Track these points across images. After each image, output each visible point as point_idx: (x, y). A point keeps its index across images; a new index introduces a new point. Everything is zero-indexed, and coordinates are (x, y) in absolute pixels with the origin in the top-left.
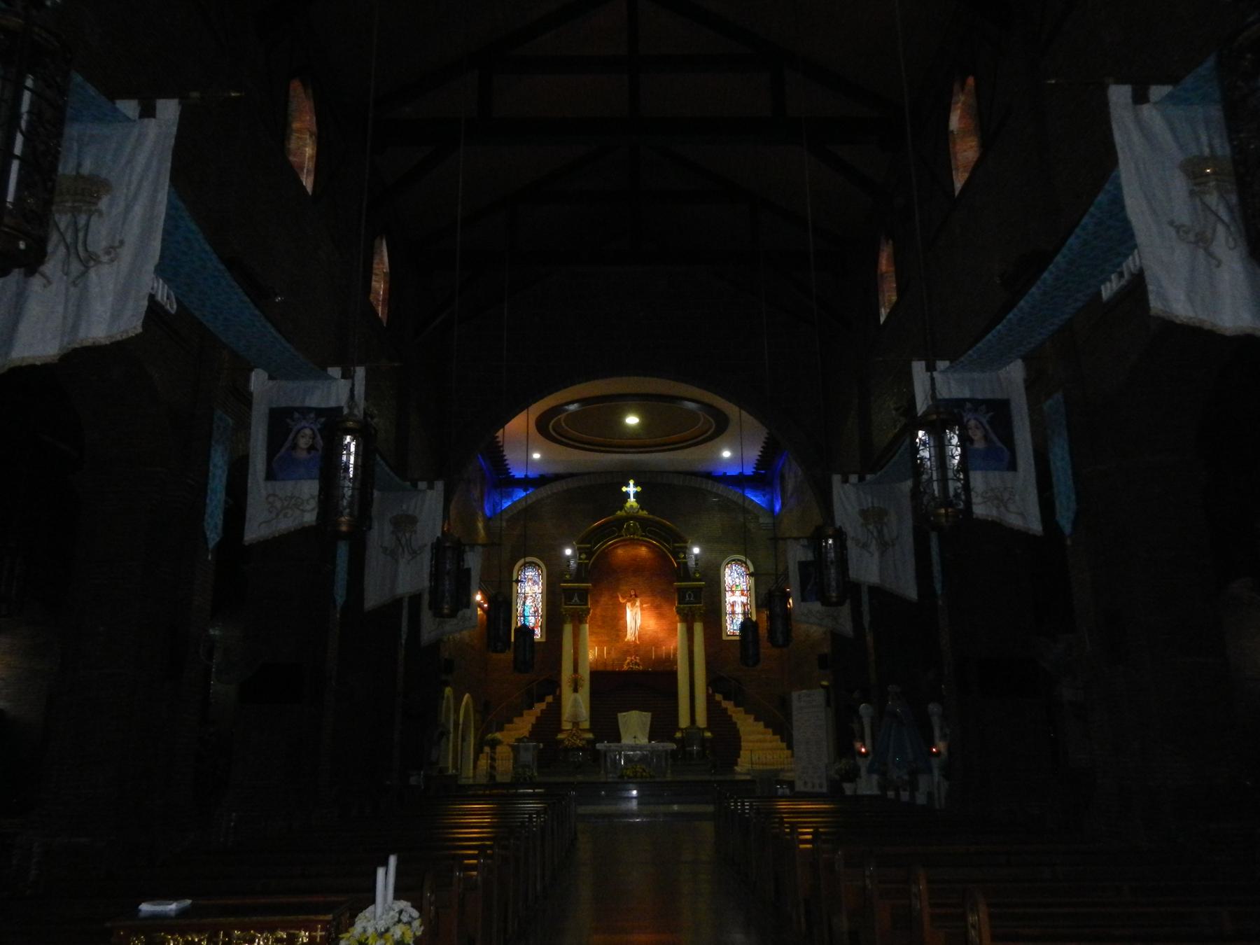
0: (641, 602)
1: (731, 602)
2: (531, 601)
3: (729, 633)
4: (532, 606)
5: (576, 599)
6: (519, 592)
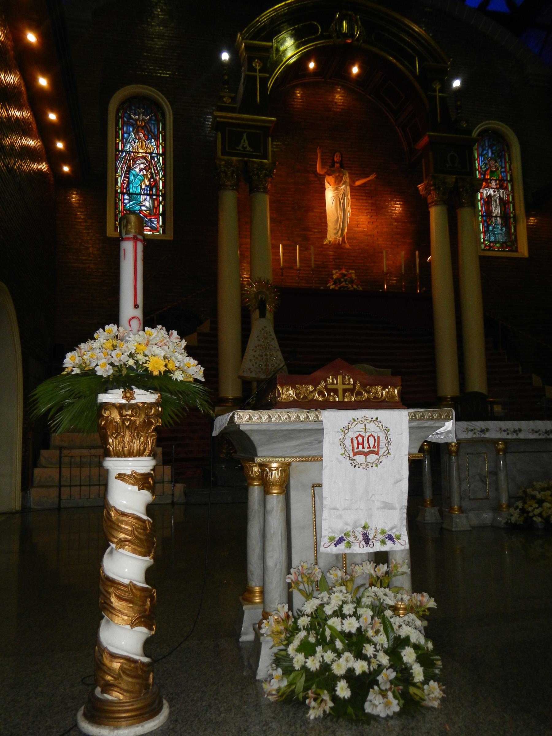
2: (142, 166)
5: (245, 142)
6: (120, 149)
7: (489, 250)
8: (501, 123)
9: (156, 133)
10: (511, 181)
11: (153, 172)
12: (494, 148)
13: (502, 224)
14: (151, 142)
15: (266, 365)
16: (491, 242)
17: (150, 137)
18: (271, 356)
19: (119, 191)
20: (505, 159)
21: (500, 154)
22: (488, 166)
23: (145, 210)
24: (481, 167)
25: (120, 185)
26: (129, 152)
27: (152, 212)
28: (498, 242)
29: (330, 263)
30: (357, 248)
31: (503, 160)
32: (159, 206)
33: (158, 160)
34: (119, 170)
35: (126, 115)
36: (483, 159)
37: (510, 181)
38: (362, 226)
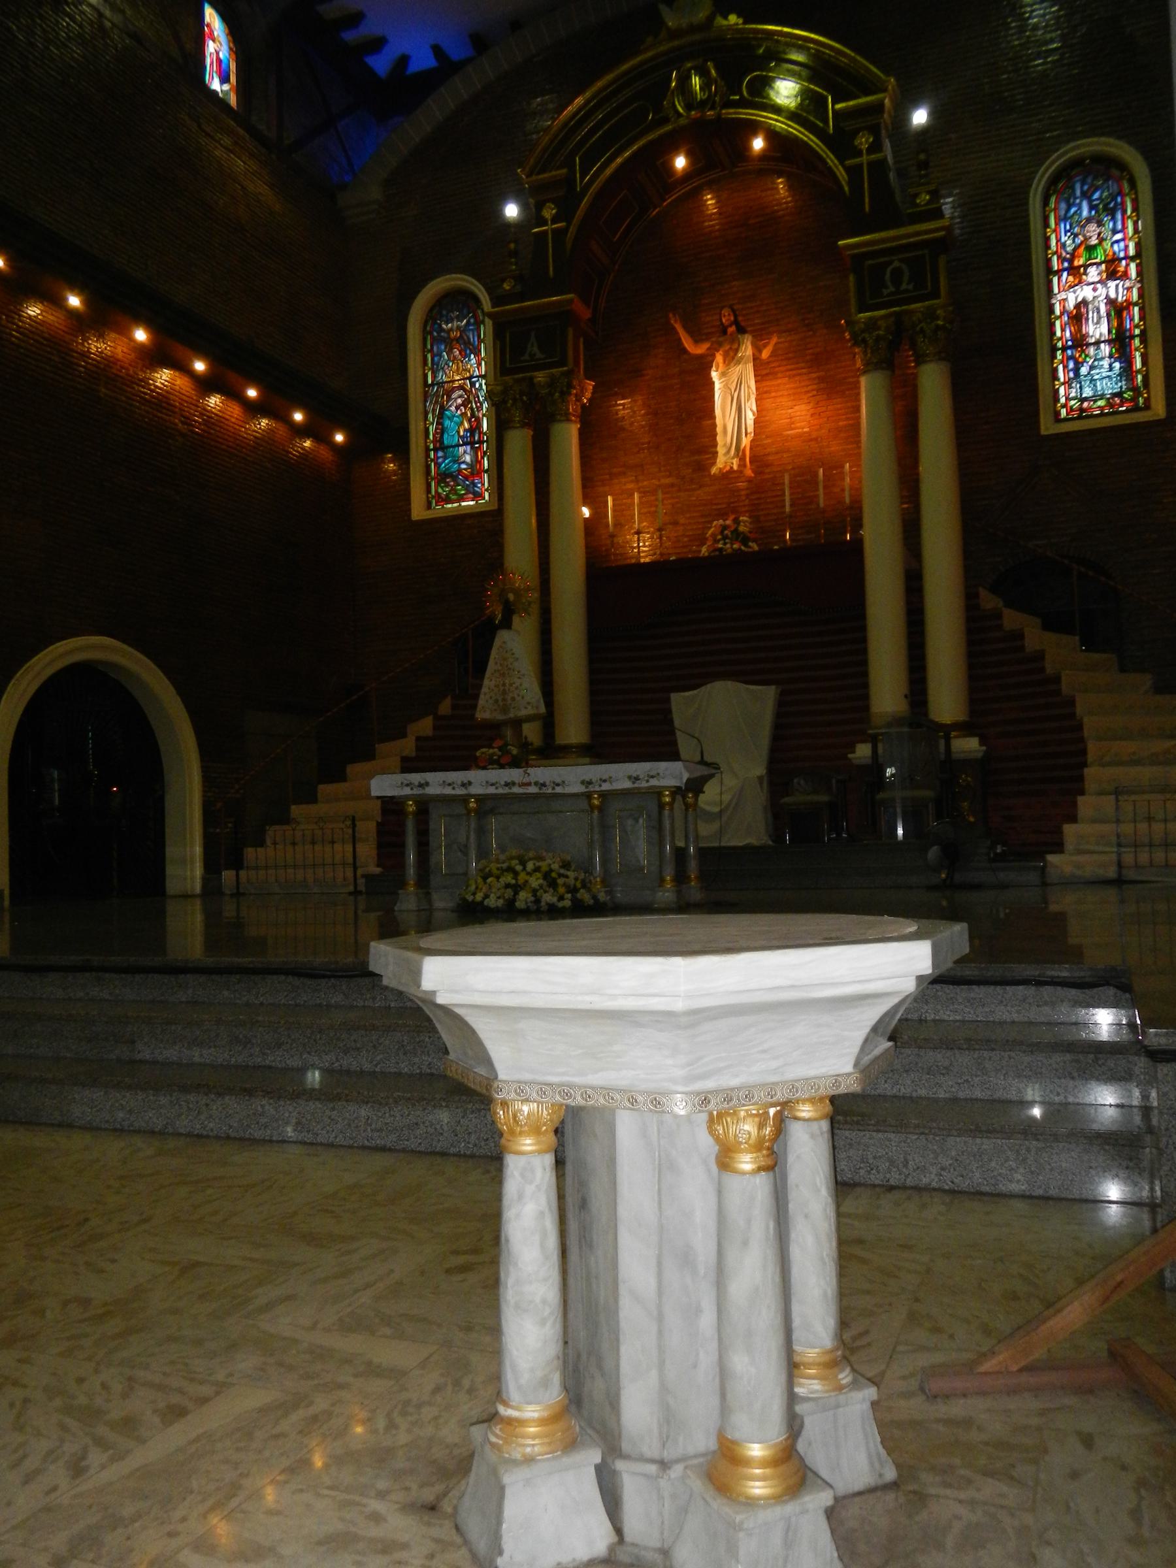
0: (753, 344)
1: (1071, 305)
2: (459, 401)
3: (1064, 412)
4: (464, 415)
5: (534, 348)
6: (430, 381)
7: (1080, 418)
8: (1103, 139)
9: (477, 343)
10: (1138, 255)
11: (474, 406)
12: (1096, 195)
13: (1111, 356)
14: (470, 360)
15: (504, 700)
16: (1083, 400)
17: (468, 352)
18: (511, 685)
19: (432, 446)
20: (1124, 212)
21: (1112, 205)
22: (1078, 241)
23: (465, 469)
24: (1064, 245)
25: (431, 437)
26: (441, 384)
27: (476, 470)
28: (1102, 397)
29: (741, 504)
30: (790, 467)
31: (1119, 216)
32: (483, 458)
33: (481, 385)
34: (430, 416)
35: (436, 326)
36: (1068, 227)
37: (1132, 259)
38: (798, 425)
